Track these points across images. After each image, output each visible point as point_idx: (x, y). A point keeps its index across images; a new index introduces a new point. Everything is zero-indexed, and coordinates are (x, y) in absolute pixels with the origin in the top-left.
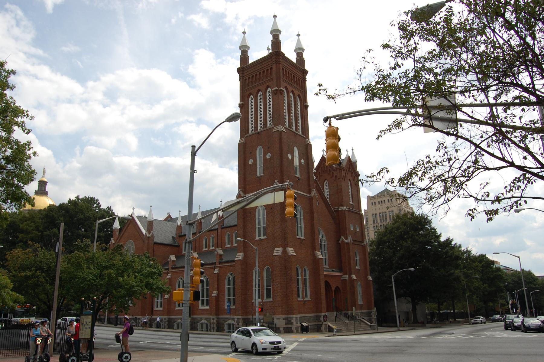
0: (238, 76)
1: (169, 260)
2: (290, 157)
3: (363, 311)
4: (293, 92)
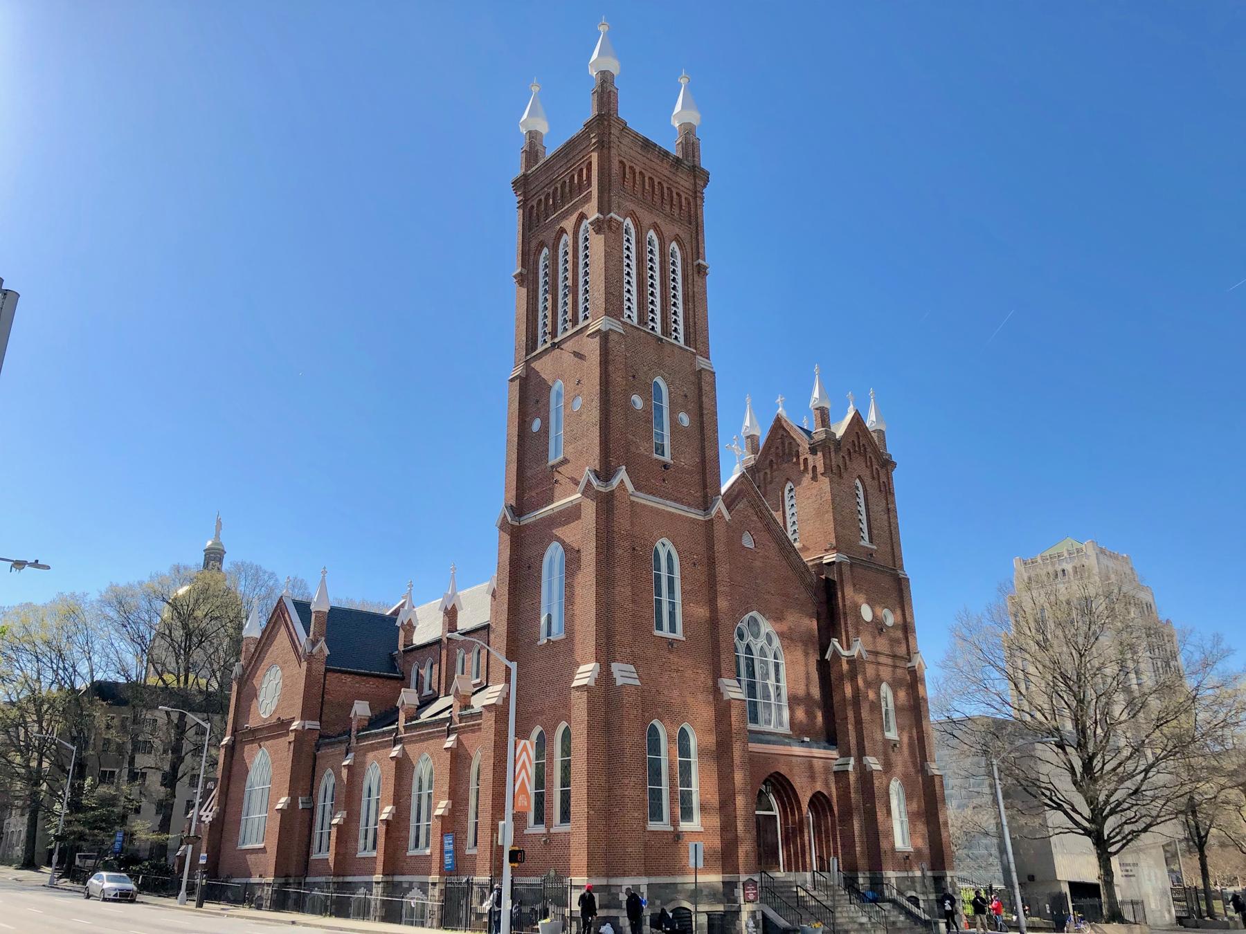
0: (514, 199)
1: (352, 715)
2: (638, 401)
3: (244, 880)
4: (656, 227)
